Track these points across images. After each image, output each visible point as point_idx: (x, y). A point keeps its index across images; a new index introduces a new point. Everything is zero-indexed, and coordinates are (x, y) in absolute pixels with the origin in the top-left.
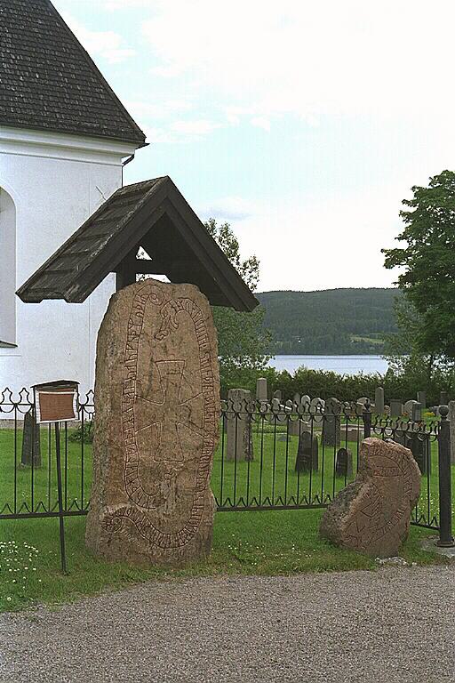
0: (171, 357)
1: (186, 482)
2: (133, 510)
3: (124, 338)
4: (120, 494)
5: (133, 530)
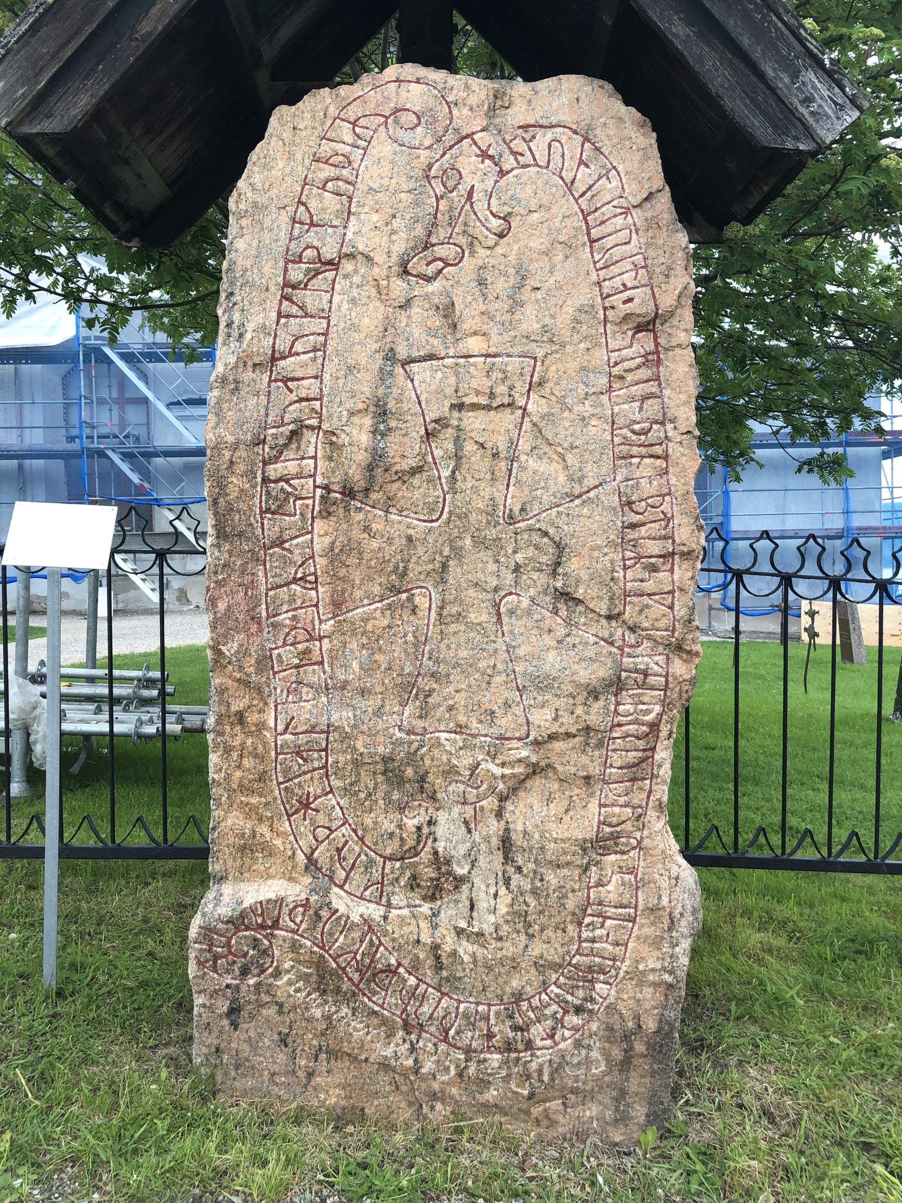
0: (474, 344)
2: (316, 912)
3: (271, 272)
4: (269, 851)
5: (324, 979)
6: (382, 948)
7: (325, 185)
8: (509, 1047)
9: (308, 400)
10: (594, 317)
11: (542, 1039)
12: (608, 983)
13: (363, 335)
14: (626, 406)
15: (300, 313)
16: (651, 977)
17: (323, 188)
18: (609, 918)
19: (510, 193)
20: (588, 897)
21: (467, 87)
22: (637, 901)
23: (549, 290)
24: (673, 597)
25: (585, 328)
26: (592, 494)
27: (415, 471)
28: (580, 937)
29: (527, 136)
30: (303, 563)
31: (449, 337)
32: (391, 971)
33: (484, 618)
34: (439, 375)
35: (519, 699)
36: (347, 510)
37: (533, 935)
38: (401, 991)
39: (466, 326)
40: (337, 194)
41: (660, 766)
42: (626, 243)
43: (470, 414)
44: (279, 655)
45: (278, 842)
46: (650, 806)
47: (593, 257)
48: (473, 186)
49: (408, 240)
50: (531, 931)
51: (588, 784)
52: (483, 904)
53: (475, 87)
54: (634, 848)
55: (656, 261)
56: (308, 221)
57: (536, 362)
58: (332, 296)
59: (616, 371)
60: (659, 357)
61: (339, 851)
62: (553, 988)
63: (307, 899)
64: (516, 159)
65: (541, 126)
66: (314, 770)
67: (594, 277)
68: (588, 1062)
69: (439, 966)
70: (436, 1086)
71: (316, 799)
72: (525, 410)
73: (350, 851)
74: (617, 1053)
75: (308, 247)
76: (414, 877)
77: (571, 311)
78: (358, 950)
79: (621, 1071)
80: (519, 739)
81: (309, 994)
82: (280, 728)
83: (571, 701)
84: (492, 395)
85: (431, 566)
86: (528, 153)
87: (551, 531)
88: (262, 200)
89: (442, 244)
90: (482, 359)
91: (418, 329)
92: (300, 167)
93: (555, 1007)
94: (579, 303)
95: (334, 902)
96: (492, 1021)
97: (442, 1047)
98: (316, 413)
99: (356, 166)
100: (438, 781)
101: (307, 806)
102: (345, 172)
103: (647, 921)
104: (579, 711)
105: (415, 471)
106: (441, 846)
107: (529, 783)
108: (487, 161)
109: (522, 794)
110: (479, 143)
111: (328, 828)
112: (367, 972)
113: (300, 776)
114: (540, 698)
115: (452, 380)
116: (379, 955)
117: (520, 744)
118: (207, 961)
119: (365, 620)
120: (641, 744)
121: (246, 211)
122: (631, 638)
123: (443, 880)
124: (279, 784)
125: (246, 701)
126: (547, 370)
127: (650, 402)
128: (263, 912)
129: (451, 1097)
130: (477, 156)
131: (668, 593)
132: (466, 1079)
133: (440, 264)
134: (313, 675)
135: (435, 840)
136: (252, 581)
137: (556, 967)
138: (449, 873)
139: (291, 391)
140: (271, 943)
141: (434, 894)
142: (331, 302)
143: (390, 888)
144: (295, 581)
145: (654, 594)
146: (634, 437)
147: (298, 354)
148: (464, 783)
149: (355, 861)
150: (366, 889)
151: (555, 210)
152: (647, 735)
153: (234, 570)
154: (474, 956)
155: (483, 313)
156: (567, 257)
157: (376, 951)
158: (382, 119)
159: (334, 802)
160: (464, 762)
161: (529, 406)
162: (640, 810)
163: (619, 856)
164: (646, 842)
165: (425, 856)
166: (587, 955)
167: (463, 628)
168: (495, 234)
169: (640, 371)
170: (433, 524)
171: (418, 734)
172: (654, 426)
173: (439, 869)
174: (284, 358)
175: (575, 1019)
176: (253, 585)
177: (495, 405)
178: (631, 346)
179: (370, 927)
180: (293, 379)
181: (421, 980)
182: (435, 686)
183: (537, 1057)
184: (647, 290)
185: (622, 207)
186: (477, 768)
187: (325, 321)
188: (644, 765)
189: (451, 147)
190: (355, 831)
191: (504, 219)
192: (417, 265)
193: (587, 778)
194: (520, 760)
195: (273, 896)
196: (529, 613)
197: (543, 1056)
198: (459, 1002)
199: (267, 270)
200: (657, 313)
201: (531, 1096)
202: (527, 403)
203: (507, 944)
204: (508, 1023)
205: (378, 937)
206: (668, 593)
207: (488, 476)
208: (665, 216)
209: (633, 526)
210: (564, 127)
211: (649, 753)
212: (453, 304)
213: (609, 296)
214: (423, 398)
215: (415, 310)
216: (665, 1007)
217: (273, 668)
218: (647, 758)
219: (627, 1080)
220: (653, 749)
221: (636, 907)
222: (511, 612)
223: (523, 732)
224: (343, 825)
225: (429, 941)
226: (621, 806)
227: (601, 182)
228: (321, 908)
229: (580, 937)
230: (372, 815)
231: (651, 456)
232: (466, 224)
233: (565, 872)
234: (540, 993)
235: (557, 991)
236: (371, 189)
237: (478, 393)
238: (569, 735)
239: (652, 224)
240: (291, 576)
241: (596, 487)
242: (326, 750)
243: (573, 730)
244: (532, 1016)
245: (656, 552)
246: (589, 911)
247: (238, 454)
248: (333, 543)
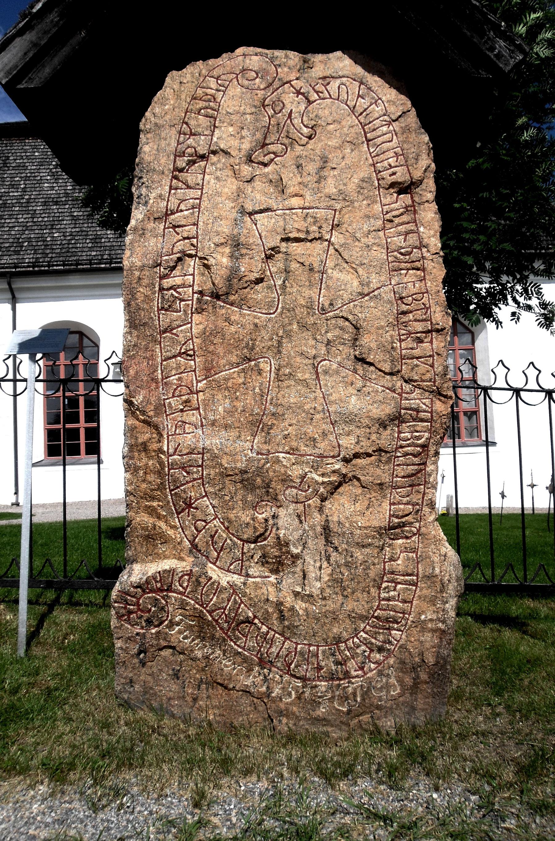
0: (295, 202)
2: (197, 580)
3: (165, 163)
4: (166, 540)
5: (203, 628)
6: (242, 605)
7: (199, 112)
8: (332, 677)
9: (188, 238)
10: (372, 185)
11: (355, 671)
12: (400, 630)
13: (223, 199)
14: (395, 238)
15: (184, 186)
16: (430, 626)
17: (199, 113)
18: (399, 583)
19: (315, 114)
20: (384, 569)
21: (286, 56)
22: (418, 571)
23: (342, 169)
24: (433, 359)
25: (366, 191)
26: (376, 293)
27: (259, 281)
28: (379, 597)
29: (325, 83)
30: (186, 343)
31: (279, 198)
32: (249, 622)
33: (307, 376)
34: (273, 220)
35: (332, 430)
36: (214, 307)
37: (347, 596)
38: (257, 637)
39: (289, 191)
40: (207, 117)
41: (430, 475)
42: (389, 142)
43: (294, 244)
44: (170, 403)
45: (171, 532)
46: (425, 504)
47: (369, 150)
48: (292, 110)
49: (251, 142)
50: (345, 593)
51: (382, 489)
54: (415, 534)
55: (409, 151)
56: (189, 133)
57: (335, 212)
58: (204, 176)
59: (388, 217)
60: (415, 209)
61: (212, 537)
62: (362, 633)
63: (191, 570)
64: (318, 95)
65: (333, 77)
67: (371, 161)
68: (388, 687)
69: (282, 618)
70: (282, 706)
71: (196, 501)
72: (329, 242)
74: (408, 681)
75: (189, 147)
76: (264, 556)
77: (356, 181)
78: (226, 606)
79: (411, 694)
80: (333, 457)
82: (171, 451)
83: (368, 430)
84: (308, 232)
85: (270, 343)
86: (326, 92)
87: (350, 317)
88: (160, 122)
89: (273, 144)
90: (301, 210)
91: (258, 195)
92: (184, 103)
93: (363, 647)
94: (361, 176)
95: (209, 572)
96: (321, 658)
97: (286, 678)
98: (194, 247)
99: (219, 101)
100: (279, 487)
102: (211, 104)
103: (426, 585)
104: (374, 437)
105: (259, 281)
106: (282, 533)
107: (341, 490)
108: (300, 96)
109: (335, 496)
110: (295, 86)
111: (205, 521)
112: (232, 623)
113: (184, 484)
114: (347, 429)
115: (281, 223)
116: (241, 610)
117: (333, 461)
118: (123, 615)
119: (226, 380)
120: (416, 460)
121: (150, 129)
122: (407, 387)
123: (284, 557)
124: (171, 491)
125: (148, 436)
126: (343, 217)
127: (410, 235)
128: (161, 580)
129: (294, 714)
130: (294, 93)
131: (430, 356)
132: (303, 701)
133: (272, 156)
134: (193, 417)
135: (278, 529)
136: (152, 355)
137: (364, 618)
138: (288, 552)
139: (178, 234)
140: (167, 602)
141: (278, 568)
142: (203, 180)
143: (247, 563)
144: (180, 354)
145: (420, 357)
146: (402, 257)
147: (182, 211)
148: (296, 488)
149: (223, 544)
150: (231, 565)
151: (344, 123)
152: (420, 454)
153: (140, 349)
154: (306, 610)
155: (300, 183)
156: (352, 150)
157: (239, 608)
158: (235, 76)
159: (208, 503)
160: (296, 472)
161: (332, 239)
162: (418, 507)
163: (404, 541)
164: (423, 530)
165: (271, 540)
166: (385, 610)
167: (293, 383)
168: (306, 137)
169: (403, 216)
170: (272, 316)
171: (264, 455)
172: (414, 250)
173: (281, 549)
174: (175, 213)
175: (378, 656)
176: (153, 357)
177: (310, 238)
178: (396, 202)
179: (234, 591)
180: (179, 226)
181: (270, 628)
182: (275, 422)
183: (353, 683)
184: (405, 168)
185: (385, 121)
186: (305, 477)
187: (200, 191)
188: (419, 475)
189: (278, 89)
190: (222, 523)
191: (312, 128)
192: (258, 156)
193: (381, 484)
194: (334, 472)
195: (167, 568)
196: (337, 372)
197: (357, 682)
199: (163, 161)
200: (412, 182)
201: (349, 712)
202: (331, 237)
203: (329, 602)
204: (332, 659)
205: (239, 598)
206: (430, 356)
207: (307, 283)
208: (414, 125)
209: (404, 313)
210: (348, 77)
211: (422, 467)
212: (281, 179)
213: (380, 172)
214: (263, 234)
215: (257, 183)
217: (166, 412)
218: (421, 470)
219: (416, 700)
220: (425, 464)
221: (417, 575)
222: (326, 372)
223: (336, 452)
224: (214, 519)
225: (275, 600)
226: (405, 504)
227: (372, 107)
228: (200, 576)
229: (379, 597)
230: (234, 512)
231: (413, 269)
232: (288, 132)
233: (367, 550)
234: (353, 638)
235: (365, 635)
236: (228, 112)
237: (299, 230)
239: (406, 130)
240: (178, 351)
241: (379, 288)
243: (370, 451)
244: (348, 654)
245: (420, 329)
246: (385, 579)
247: (144, 273)
248: (205, 329)
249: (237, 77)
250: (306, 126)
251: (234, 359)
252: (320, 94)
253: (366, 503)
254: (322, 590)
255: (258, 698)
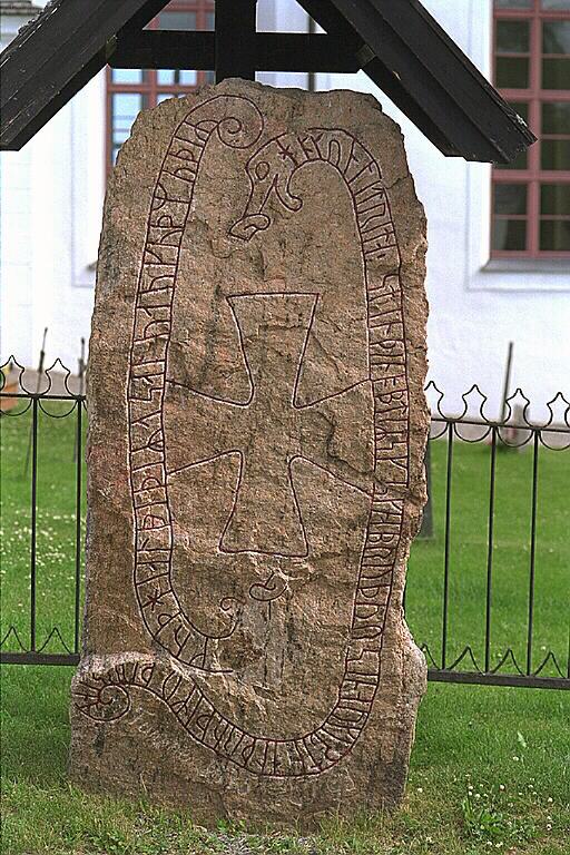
0: (276, 285)
1: (313, 608)
5: (162, 719)
15: (157, 261)
16: (389, 724)
33: (280, 473)
37: (307, 693)
50: (306, 690)
52: (274, 669)
53: (280, 103)
54: (379, 634)
61: (176, 632)
66: (161, 575)
70: (238, 799)
73: (185, 631)
76: (226, 651)
81: (152, 731)
83: (337, 531)
101: (154, 600)
124: (136, 585)
135: (242, 625)
138: (251, 648)
174: (147, 292)
188: (386, 576)
192: (238, 228)
198: (255, 738)
211: (390, 568)
216: (398, 746)
220: (393, 565)
221: (379, 675)
222: (298, 470)
232: (272, 203)
234: (311, 734)
235: (323, 732)
238: (335, 554)
242: (169, 562)
249: (218, 127)
250: (293, 197)
251: (206, 453)
252: (310, 153)
253: (331, 602)
254: (283, 686)
255: (213, 791)
